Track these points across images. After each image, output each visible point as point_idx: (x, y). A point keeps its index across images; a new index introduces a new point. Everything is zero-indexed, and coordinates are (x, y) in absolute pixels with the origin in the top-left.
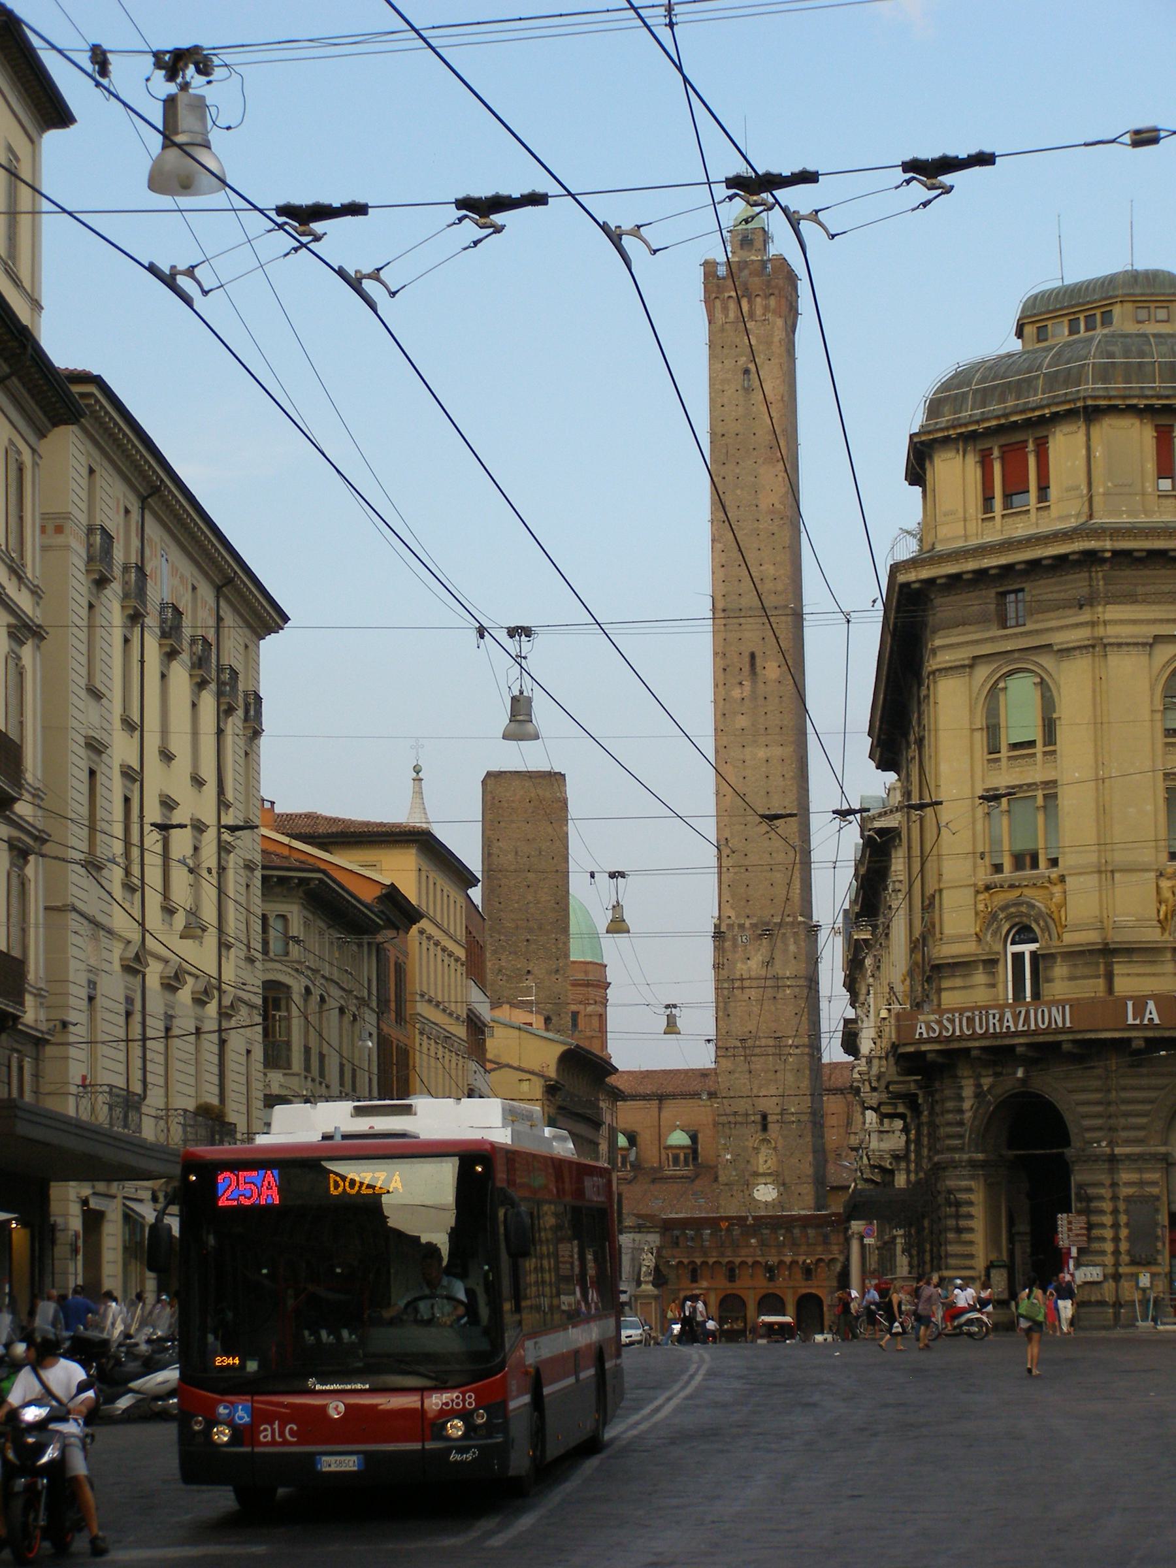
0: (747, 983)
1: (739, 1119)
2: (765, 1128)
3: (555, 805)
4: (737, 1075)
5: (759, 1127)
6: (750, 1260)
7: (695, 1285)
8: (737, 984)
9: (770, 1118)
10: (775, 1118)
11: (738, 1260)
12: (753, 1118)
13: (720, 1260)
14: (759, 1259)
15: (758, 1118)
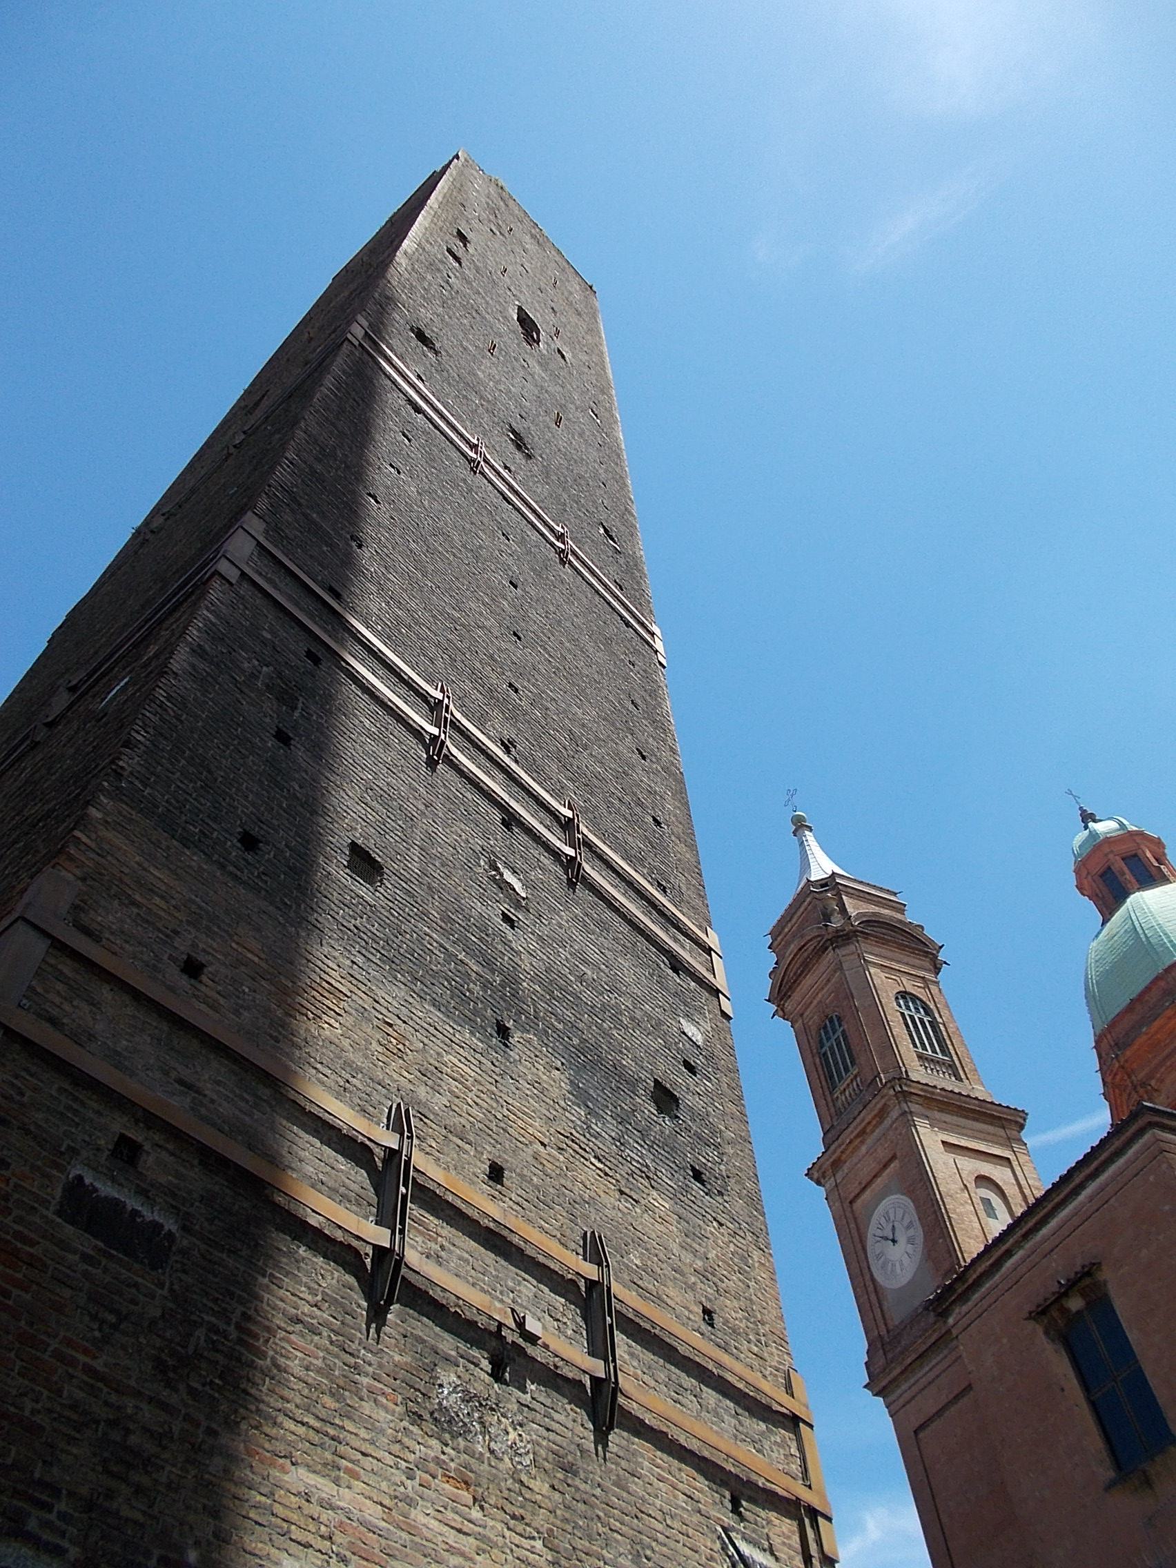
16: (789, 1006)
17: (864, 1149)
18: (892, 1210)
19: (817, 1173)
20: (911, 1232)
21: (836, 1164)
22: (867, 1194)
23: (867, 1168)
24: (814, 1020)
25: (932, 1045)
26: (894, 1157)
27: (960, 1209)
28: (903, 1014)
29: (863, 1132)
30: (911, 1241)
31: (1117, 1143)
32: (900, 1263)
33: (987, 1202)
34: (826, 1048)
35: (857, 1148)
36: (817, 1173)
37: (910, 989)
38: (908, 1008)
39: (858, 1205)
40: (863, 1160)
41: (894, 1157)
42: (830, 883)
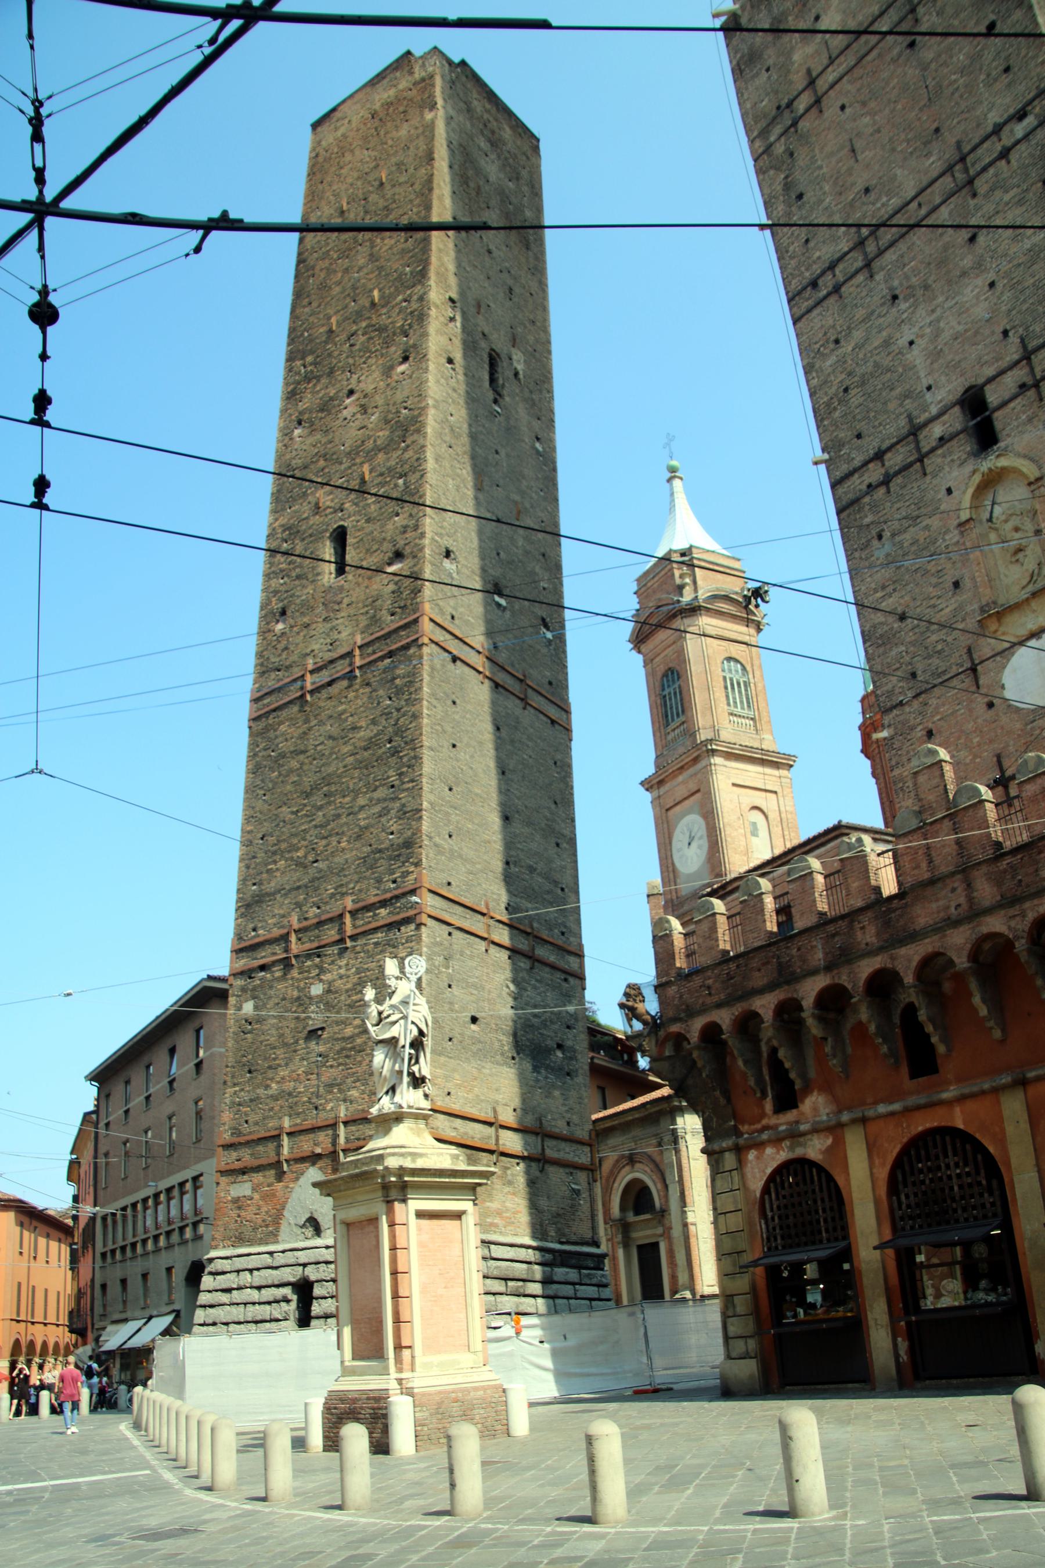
0: (822, 84)
1: (895, 460)
2: (985, 437)
3: (414, 92)
4: (858, 335)
5: (963, 446)
6: (958, 943)
7: (791, 1116)
8: (801, 105)
9: (993, 397)
10: (1010, 381)
11: (907, 960)
12: (937, 430)
13: (844, 979)
14: (995, 924)
15: (955, 420)
16: (643, 648)
17: (680, 778)
18: (690, 823)
19: (648, 785)
20: (701, 842)
21: (661, 783)
22: (678, 808)
23: (681, 792)
24: (661, 669)
25: (742, 702)
26: (698, 791)
27: (734, 834)
28: (725, 678)
29: (682, 768)
30: (700, 847)
31: (823, 840)
32: (691, 859)
33: (754, 824)
34: (666, 692)
35: (675, 777)
36: (648, 785)
37: (734, 655)
38: (730, 671)
39: (671, 813)
40: (679, 786)
41: (698, 791)
42: (687, 558)
